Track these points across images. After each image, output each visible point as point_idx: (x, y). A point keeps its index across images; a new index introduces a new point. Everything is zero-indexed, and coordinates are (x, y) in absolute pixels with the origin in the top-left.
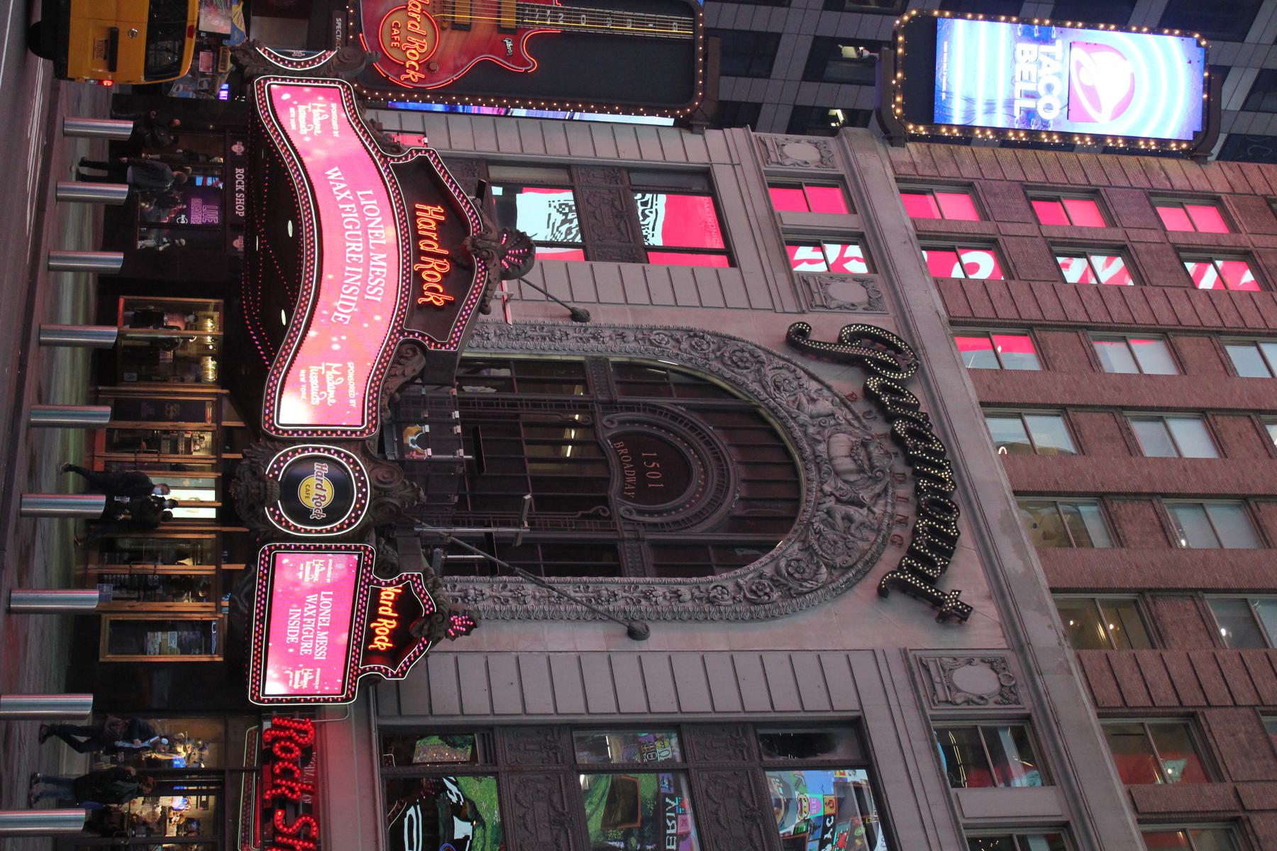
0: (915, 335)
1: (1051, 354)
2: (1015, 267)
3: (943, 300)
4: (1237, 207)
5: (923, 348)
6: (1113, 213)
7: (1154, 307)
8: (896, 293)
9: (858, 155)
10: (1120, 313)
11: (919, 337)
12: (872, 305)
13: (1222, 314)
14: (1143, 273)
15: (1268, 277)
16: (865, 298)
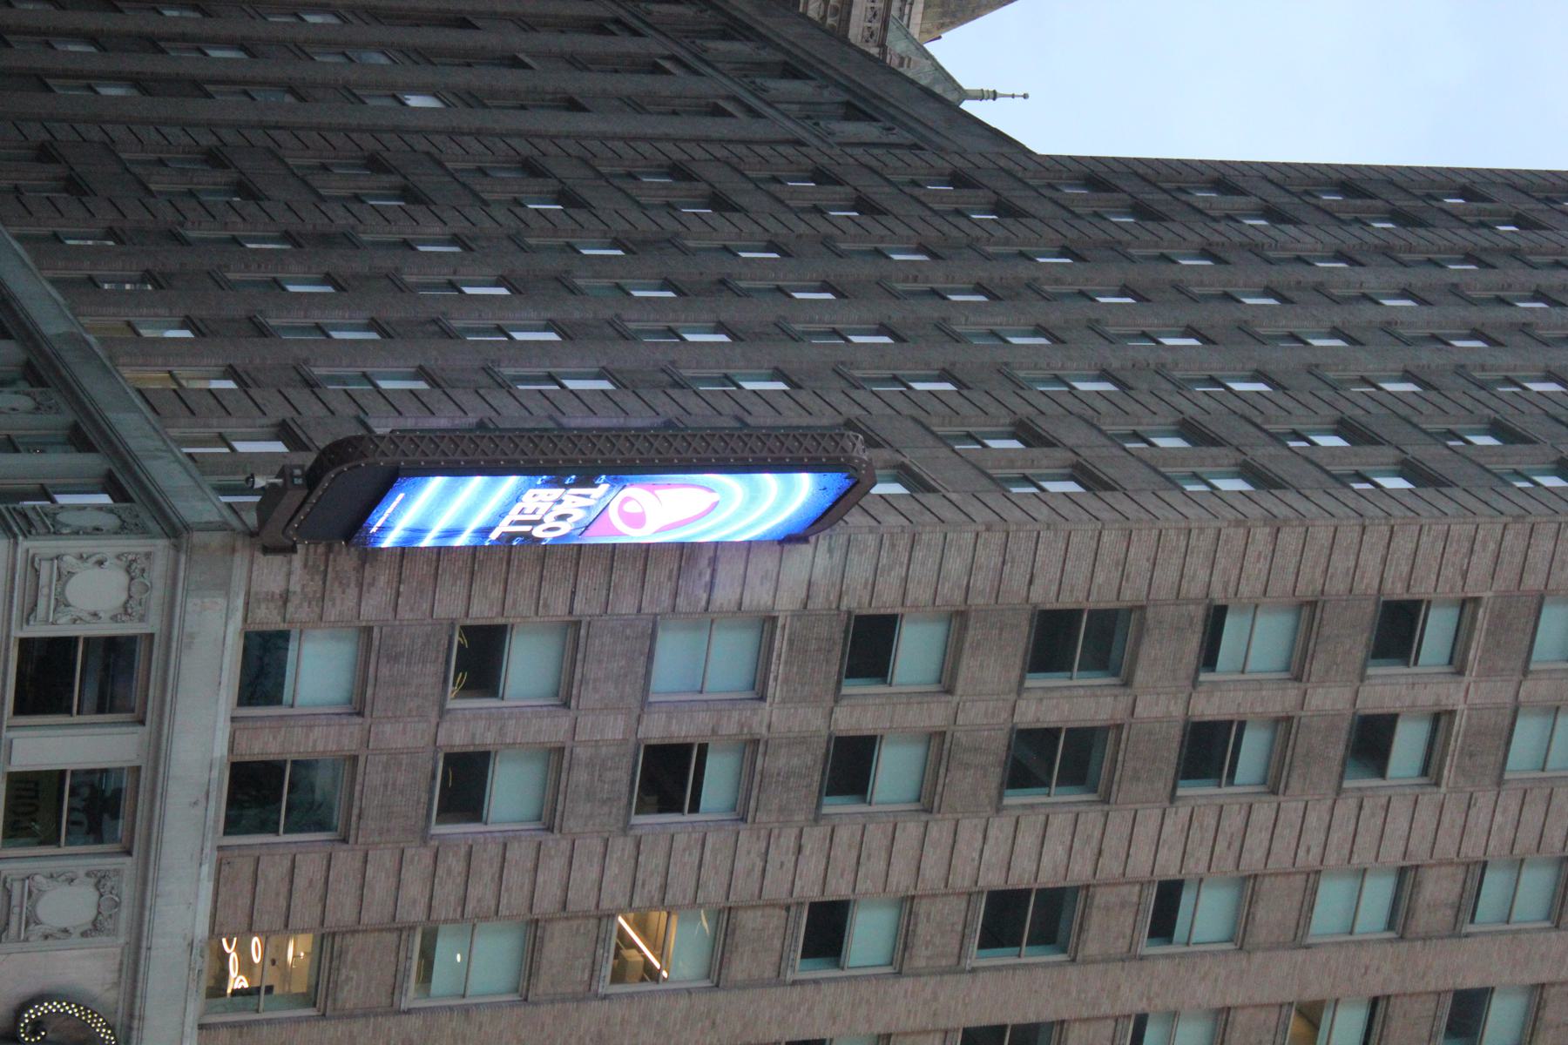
0: (139, 993)
1: (343, 977)
2: (360, 817)
3: (215, 901)
4: (791, 642)
5: (142, 1018)
6: (578, 676)
7: (540, 879)
8: (142, 906)
9: (193, 604)
10: (479, 901)
11: (144, 997)
12: (96, 927)
13: (639, 883)
14: (560, 808)
15: (755, 793)
16: (93, 913)
